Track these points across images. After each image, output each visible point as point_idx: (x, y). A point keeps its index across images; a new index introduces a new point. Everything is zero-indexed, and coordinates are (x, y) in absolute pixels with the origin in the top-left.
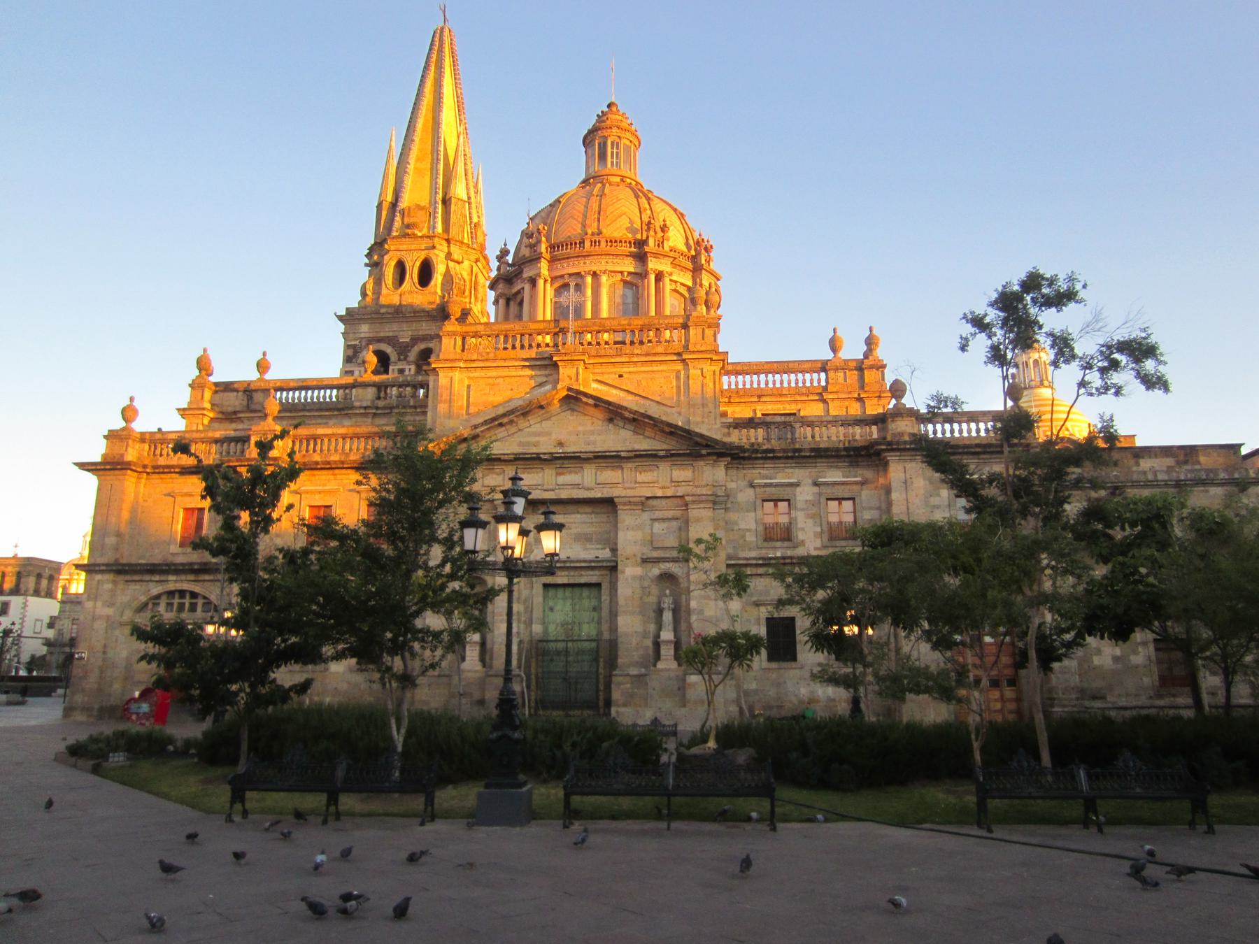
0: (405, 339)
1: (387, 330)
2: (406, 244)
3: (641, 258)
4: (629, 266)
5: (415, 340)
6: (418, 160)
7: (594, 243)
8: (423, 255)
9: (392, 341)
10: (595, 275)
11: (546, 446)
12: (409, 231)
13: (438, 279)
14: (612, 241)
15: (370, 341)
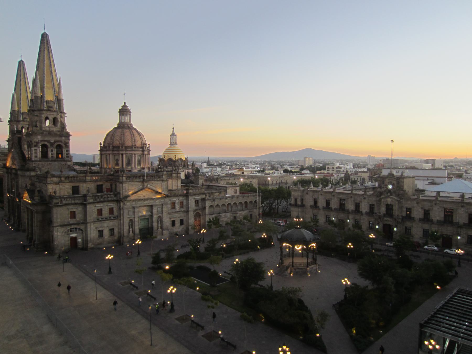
0: (52, 141)
1: (46, 138)
2: (49, 113)
3: (143, 151)
4: (141, 153)
5: (55, 142)
6: (47, 83)
7: (134, 148)
8: (55, 116)
9: (48, 141)
10: (135, 154)
11: (142, 197)
12: (50, 109)
13: (59, 124)
14: (138, 147)
15: (42, 141)
